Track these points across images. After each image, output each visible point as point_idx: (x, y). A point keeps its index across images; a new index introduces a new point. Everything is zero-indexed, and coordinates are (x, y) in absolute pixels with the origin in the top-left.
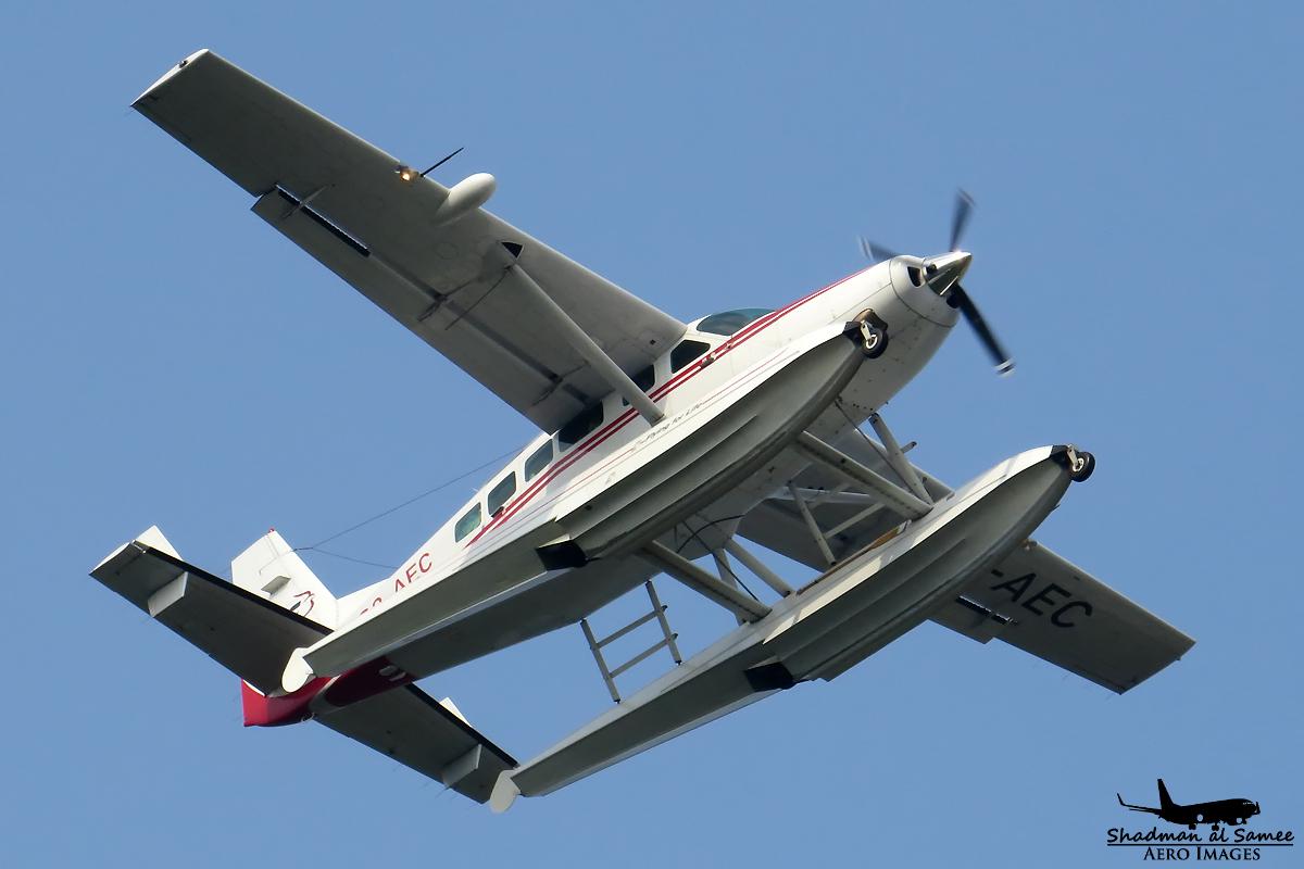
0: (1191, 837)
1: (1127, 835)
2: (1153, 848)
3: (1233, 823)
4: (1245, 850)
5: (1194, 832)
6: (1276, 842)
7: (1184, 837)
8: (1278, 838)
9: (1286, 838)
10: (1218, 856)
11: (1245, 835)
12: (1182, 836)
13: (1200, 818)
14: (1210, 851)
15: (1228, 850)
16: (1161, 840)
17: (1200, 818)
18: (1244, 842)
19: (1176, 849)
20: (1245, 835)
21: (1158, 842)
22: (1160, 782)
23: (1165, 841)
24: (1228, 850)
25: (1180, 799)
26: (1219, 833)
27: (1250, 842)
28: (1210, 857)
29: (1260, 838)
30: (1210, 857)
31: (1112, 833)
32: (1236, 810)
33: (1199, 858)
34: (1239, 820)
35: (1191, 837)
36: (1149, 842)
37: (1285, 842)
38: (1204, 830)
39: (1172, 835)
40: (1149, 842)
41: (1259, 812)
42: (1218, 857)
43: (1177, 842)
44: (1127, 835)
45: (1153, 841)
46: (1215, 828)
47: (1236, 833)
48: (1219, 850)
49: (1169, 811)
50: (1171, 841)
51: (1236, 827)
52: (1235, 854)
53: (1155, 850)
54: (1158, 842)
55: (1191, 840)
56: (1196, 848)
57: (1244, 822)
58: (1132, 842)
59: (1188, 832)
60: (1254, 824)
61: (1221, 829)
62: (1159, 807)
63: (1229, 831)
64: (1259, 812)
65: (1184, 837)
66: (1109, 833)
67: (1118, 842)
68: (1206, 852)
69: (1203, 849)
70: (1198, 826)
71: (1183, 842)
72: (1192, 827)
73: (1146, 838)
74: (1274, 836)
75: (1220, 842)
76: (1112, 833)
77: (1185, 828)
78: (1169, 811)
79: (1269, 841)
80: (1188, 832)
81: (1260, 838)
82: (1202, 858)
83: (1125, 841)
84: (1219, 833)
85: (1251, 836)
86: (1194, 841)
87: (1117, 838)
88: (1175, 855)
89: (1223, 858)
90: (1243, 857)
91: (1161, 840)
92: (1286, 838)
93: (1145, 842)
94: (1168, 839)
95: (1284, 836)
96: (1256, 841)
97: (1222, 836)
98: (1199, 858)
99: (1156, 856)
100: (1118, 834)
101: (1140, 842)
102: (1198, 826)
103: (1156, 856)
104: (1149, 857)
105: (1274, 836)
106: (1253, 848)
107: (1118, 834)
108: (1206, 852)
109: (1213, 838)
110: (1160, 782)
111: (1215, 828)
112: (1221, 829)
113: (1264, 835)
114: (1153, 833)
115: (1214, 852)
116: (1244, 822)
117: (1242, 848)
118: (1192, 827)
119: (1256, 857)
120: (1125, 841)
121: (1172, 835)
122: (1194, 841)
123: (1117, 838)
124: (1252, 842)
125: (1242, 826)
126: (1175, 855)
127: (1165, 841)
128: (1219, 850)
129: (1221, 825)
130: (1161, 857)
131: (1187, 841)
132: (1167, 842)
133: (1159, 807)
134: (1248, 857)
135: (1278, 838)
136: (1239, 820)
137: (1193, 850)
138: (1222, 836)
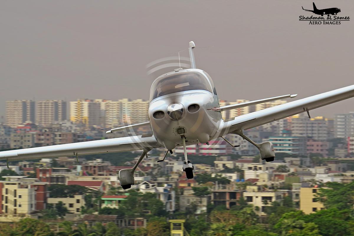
0: (322, 18)
1: (305, 18)
2: (311, 21)
3: (333, 14)
4: (337, 22)
5: (323, 17)
6: (345, 19)
7: (320, 18)
8: (345, 18)
9: (348, 19)
10: (329, 23)
11: (336, 17)
12: (320, 18)
13: (324, 13)
14: (327, 22)
15: (332, 22)
16: (314, 19)
17: (324, 13)
18: (336, 19)
19: (318, 21)
20: (336, 17)
21: (313, 19)
22: (313, 3)
23: (315, 19)
24: (332, 22)
25: (319, 8)
26: (329, 17)
27: (338, 20)
28: (327, 24)
29: (341, 18)
30: (327, 24)
31: (300, 17)
32: (334, 11)
33: (324, 24)
34: (335, 14)
35: (322, 18)
36: (311, 20)
37: (347, 19)
38: (325, 16)
39: (317, 18)
40: (311, 20)
41: (340, 11)
42: (329, 23)
43: (318, 19)
44: (305, 18)
45: (311, 19)
46: (328, 16)
47: (334, 17)
48: (329, 22)
49: (316, 11)
50: (316, 19)
51: (334, 16)
52: (334, 23)
53: (312, 22)
54: (313, 19)
55: (322, 19)
56: (323, 21)
57: (336, 14)
58: (306, 19)
59: (321, 17)
60: (339, 15)
61: (330, 16)
62: (313, 10)
63: (332, 16)
64: (340, 11)
65: (320, 18)
66: (300, 17)
67: (302, 19)
68: (326, 22)
69: (325, 21)
70: (324, 15)
71: (320, 19)
72: (322, 15)
73: (310, 18)
74: (344, 18)
75: (330, 19)
76: (300, 17)
77: (320, 16)
78: (316, 11)
79: (343, 19)
80: (321, 17)
81: (341, 18)
82: (325, 24)
83: (304, 19)
84: (329, 17)
85: (338, 18)
86: (323, 19)
87: (302, 18)
88: (318, 23)
89: (331, 24)
90: (336, 23)
91: (314, 19)
92: (348, 19)
93: (309, 19)
94: (316, 19)
95: (347, 18)
96: (340, 19)
97: (330, 18)
98: (324, 24)
99: (312, 23)
100: (302, 17)
101: (308, 19)
102: (324, 15)
103: (312, 23)
104: (311, 24)
105: (344, 18)
106: (339, 21)
107: (302, 17)
108: (326, 22)
109: (328, 18)
110: (313, 3)
111: (328, 16)
112: (330, 16)
113: (342, 18)
114: (312, 17)
115: (328, 22)
116: (336, 14)
117: (336, 21)
118: (322, 15)
119: (340, 24)
120: (304, 19)
121: (317, 18)
122: (323, 19)
123: (302, 18)
124: (338, 19)
125: (336, 15)
126: (318, 23)
127: (315, 19)
128: (329, 22)
129: (330, 15)
130: (314, 23)
131: (321, 19)
132: (315, 20)
133: (313, 10)
134: (337, 23)
135: (345, 18)
136: (335, 14)
137: (322, 22)
138: (330, 18)
